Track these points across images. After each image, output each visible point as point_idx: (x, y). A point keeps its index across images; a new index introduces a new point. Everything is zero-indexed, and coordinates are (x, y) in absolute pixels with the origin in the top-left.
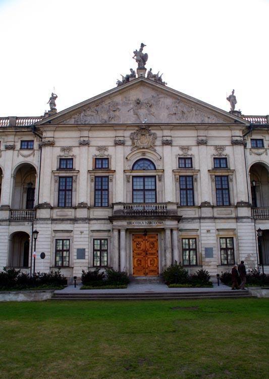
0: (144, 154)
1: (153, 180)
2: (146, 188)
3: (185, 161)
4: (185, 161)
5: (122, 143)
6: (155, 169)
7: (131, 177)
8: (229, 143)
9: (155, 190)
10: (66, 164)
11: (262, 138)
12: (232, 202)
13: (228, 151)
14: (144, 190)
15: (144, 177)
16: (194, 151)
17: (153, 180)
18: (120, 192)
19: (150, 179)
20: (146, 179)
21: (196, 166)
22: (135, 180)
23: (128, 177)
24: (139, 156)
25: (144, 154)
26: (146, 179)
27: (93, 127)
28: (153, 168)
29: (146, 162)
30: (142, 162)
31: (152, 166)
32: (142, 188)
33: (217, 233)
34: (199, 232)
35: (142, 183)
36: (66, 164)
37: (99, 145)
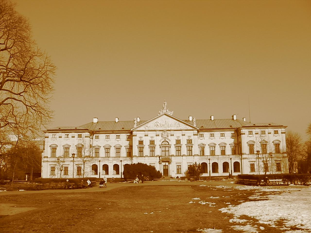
0: (165, 139)
1: (168, 148)
2: (166, 150)
3: (178, 142)
4: (178, 142)
5: (159, 135)
6: (169, 144)
7: (161, 147)
9: (169, 151)
10: (141, 142)
11: (203, 133)
12: (192, 155)
13: (193, 138)
14: (165, 151)
15: (165, 147)
16: (181, 138)
17: (168, 148)
18: (158, 151)
19: (167, 148)
21: (181, 143)
22: (162, 148)
23: (160, 147)
24: (164, 140)
25: (165, 139)
26: (166, 148)
28: (168, 144)
29: (166, 142)
30: (165, 142)
31: (168, 143)
32: (165, 150)
33: (187, 164)
34: (182, 164)
35: (165, 149)
36: (141, 142)
37: (152, 136)
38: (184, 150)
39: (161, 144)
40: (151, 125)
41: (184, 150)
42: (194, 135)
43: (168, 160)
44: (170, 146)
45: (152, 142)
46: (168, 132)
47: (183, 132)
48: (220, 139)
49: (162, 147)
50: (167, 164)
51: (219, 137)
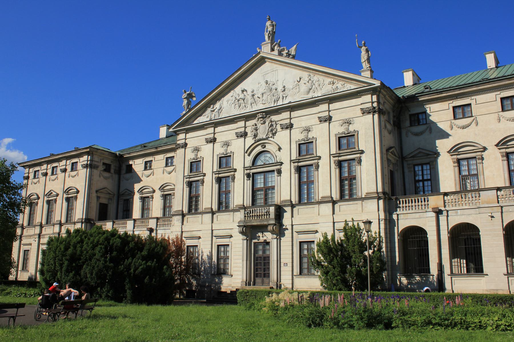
3: (305, 147)
5: (244, 135)
8: (359, 113)
20: (267, 174)
23: (248, 175)
24: (259, 149)
27: (216, 124)
38: (326, 181)
39: (248, 163)
40: (227, 106)
41: (326, 181)
42: (365, 112)
43: (265, 223)
44: (278, 167)
45: (224, 160)
46: (274, 118)
47: (324, 107)
48: (499, 120)
49: (253, 174)
50: (268, 236)
51: (496, 114)
